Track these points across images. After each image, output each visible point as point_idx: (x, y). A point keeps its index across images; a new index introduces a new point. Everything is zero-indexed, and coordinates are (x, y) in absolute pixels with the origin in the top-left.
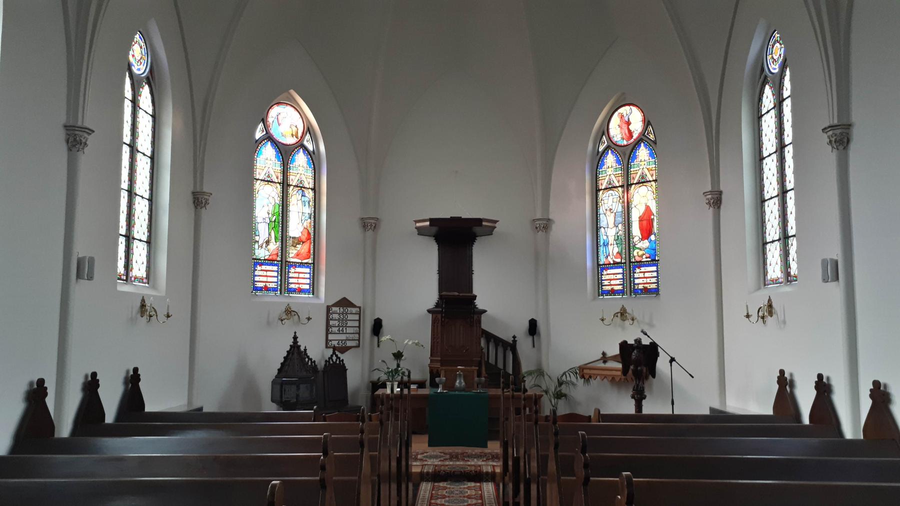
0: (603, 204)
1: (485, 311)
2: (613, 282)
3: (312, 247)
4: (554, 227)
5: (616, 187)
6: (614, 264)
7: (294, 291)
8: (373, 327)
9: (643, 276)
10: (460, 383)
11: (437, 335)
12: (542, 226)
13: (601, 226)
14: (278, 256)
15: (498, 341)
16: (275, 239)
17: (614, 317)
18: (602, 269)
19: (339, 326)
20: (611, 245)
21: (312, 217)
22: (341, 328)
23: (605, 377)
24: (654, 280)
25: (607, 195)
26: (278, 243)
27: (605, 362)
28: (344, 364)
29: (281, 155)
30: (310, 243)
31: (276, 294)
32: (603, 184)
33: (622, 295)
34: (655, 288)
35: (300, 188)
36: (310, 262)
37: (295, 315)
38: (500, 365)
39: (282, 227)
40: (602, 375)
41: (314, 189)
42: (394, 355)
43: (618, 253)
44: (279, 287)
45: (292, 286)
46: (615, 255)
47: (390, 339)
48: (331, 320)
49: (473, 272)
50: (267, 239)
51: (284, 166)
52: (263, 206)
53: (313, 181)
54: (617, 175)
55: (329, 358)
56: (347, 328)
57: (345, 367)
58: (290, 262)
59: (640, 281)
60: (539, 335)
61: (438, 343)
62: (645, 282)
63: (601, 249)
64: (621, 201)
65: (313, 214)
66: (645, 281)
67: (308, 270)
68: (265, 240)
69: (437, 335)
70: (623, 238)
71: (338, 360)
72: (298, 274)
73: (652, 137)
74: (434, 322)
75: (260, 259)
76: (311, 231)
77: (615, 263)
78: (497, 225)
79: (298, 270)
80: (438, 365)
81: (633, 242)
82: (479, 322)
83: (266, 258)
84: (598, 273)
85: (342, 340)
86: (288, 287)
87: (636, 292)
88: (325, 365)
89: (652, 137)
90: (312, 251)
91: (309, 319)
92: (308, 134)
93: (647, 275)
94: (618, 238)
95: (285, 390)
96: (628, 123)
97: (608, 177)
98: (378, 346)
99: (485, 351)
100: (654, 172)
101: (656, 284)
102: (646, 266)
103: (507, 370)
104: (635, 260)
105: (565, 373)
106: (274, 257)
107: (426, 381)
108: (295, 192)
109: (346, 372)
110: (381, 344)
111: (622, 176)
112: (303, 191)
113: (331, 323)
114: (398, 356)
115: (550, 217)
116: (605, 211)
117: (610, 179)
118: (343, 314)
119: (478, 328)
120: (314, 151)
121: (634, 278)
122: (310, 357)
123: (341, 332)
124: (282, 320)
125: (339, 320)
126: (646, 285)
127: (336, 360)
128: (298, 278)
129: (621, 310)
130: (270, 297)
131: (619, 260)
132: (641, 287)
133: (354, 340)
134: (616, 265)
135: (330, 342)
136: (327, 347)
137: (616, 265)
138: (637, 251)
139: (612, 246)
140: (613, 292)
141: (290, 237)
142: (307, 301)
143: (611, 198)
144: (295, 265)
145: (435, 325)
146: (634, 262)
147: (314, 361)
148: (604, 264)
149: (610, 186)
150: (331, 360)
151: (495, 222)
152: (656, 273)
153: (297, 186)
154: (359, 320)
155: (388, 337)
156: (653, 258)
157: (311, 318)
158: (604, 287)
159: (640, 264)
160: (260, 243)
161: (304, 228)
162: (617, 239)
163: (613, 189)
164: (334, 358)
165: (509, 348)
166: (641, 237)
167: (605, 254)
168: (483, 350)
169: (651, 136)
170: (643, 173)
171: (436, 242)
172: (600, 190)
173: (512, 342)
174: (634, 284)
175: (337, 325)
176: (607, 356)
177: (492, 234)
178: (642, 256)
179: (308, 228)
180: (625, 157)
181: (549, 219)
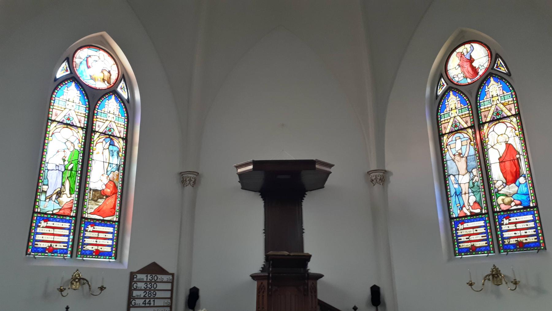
0: (449, 149)
1: (321, 276)
2: (472, 238)
3: (118, 202)
4: (391, 178)
5: (465, 129)
6: (471, 216)
7: (91, 253)
8: (188, 298)
12: (379, 178)
13: (450, 173)
14: (71, 211)
16: (70, 190)
17: (485, 280)
18: (456, 224)
19: (145, 297)
20: (465, 194)
21: (121, 168)
24: (531, 232)
25: (454, 139)
26: (73, 196)
29: (88, 98)
30: (116, 198)
31: (64, 256)
32: (447, 128)
35: (107, 136)
36: (115, 220)
37: (84, 284)
39: (81, 177)
41: (125, 139)
43: (475, 202)
45: (89, 248)
46: (471, 204)
48: (135, 289)
49: (304, 231)
50: (59, 189)
51: (89, 110)
52: (58, 152)
53: (125, 130)
54: (464, 116)
58: (87, 219)
59: (512, 234)
60: (384, 305)
62: (519, 235)
63: (453, 200)
64: (472, 143)
65: (122, 166)
66: (518, 233)
67: (111, 229)
68: (55, 192)
69: (263, 308)
70: (480, 184)
72: (97, 233)
73: (503, 70)
75: (46, 214)
77: (473, 214)
78: (332, 170)
79: (98, 228)
81: (495, 188)
82: (314, 290)
83: (55, 212)
84: (452, 228)
86: (82, 248)
87: (507, 248)
89: (503, 70)
90: (117, 208)
91: (102, 288)
92: (123, 82)
93: (519, 226)
96: (471, 60)
97: (452, 119)
100: (512, 106)
101: (536, 237)
104: (500, 209)
106: (67, 212)
108: (101, 140)
111: (470, 116)
112: (111, 139)
113: (135, 293)
115: (386, 169)
116: (453, 157)
117: (455, 122)
120: (128, 100)
121: (502, 231)
123: (147, 305)
124: (61, 291)
125: (145, 290)
126: (519, 239)
128: (97, 238)
129: (493, 271)
130: (56, 261)
131: (478, 211)
132: (513, 241)
134: (474, 217)
137: (474, 217)
139: (467, 195)
140: (474, 250)
141: (90, 189)
142: (109, 267)
143: (459, 142)
144: (94, 223)
145: (261, 293)
146: (499, 212)
148: (458, 217)
149: (456, 129)
151: (331, 166)
152: (533, 223)
153: (104, 134)
154: (172, 290)
156: (526, 204)
157: (105, 288)
158: (461, 245)
159: (508, 213)
161: (110, 180)
162: (472, 186)
163: (461, 131)
166: (505, 181)
167: (458, 205)
169: (502, 68)
170: (497, 109)
172: (443, 135)
174: (503, 239)
175: (142, 296)
177: (324, 187)
179: (115, 181)
180: (471, 96)
181: (386, 171)
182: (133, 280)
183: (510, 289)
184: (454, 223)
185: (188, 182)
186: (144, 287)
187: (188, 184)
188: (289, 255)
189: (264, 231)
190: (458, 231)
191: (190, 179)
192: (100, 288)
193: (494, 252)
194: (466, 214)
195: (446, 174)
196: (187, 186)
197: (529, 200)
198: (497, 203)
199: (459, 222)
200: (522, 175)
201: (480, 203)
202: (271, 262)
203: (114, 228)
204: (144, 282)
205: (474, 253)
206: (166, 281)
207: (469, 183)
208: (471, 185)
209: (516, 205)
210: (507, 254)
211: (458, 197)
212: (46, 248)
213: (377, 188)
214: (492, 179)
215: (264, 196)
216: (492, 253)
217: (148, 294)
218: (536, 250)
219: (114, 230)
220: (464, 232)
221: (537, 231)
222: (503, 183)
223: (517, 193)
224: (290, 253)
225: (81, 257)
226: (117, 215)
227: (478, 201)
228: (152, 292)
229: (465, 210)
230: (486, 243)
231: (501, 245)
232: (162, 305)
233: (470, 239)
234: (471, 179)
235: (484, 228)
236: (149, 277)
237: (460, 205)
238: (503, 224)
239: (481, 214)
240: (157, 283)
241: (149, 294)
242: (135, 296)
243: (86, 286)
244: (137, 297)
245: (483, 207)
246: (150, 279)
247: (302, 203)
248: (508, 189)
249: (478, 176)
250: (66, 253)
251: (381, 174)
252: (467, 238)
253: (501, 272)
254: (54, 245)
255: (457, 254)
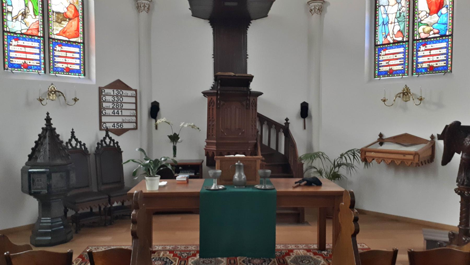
1: (261, 94)
2: (391, 63)
3: (81, 25)
6: (393, 43)
7: (62, 70)
8: (150, 110)
9: (429, 54)
10: (240, 176)
11: (213, 118)
12: (317, 8)
15: (271, 123)
16: (34, 12)
17: (396, 97)
18: (380, 51)
20: (392, 23)
22: (116, 111)
23: (383, 159)
26: (37, 17)
27: (381, 144)
28: (119, 146)
30: (78, 22)
33: (402, 76)
34: (443, 66)
36: (80, 41)
37: (60, 95)
38: (273, 146)
40: (379, 158)
42: (170, 137)
43: (399, 31)
44: (43, 66)
45: (60, 65)
46: (395, 33)
47: (166, 122)
48: (104, 102)
49: (248, 56)
50: (24, 10)
55: (102, 141)
56: (123, 111)
57: (120, 149)
58: (54, 39)
59: (425, 59)
60: (311, 117)
61: (213, 125)
62: (432, 60)
63: (380, 29)
66: (431, 58)
67: (77, 50)
69: (213, 118)
70: (406, 14)
71: (112, 142)
72: (65, 53)
74: (210, 104)
75: (15, 33)
76: (79, 8)
77: (395, 42)
79: (65, 48)
80: (214, 148)
81: (419, 18)
83: (23, 32)
84: (375, 54)
85: (118, 123)
86: (53, 66)
88: (97, 148)
90: (81, 30)
91: (76, 100)
93: (433, 52)
94: (400, 16)
95: (33, 181)
98: (156, 128)
99: (260, 133)
102: (434, 43)
103: (279, 151)
105: (342, 155)
106: (35, 32)
107: (203, 161)
109: (121, 155)
110: (159, 127)
113: (105, 105)
114: (174, 138)
118: (117, 96)
119: (254, 111)
122: (79, 140)
123: (116, 114)
124: (41, 100)
125: (113, 102)
126: (431, 64)
127: (110, 142)
128: (66, 57)
129: (404, 90)
130: (32, 76)
131: (400, 39)
132: (425, 65)
133: (131, 122)
135: (104, 125)
136: (101, 129)
138: (422, 27)
140: (391, 73)
141: (53, 12)
145: (211, 107)
146: (419, 40)
147: (84, 144)
148: (382, 45)
150: (103, 143)
154: (136, 103)
155: (163, 120)
156: (443, 33)
157: (78, 99)
159: (426, 41)
160: (14, 14)
161: (71, 4)
164: (108, 140)
165: (282, 130)
166: (428, 11)
167: (384, 33)
168: (258, 133)
171: (211, 25)
173: (284, 125)
175: (111, 107)
176: (384, 138)
177: (268, 16)
178: (428, 32)
179: (75, 4)
182: (102, 93)
183: (416, 105)
184: (378, 49)
185: (143, 8)
186: (112, 100)
187: (143, 10)
188: (234, 76)
189: (213, 56)
190: (380, 57)
191: (144, 4)
192: (74, 99)
193: (408, 75)
194: (389, 41)
195: (377, 4)
196: (142, 12)
197: (446, 28)
198: (418, 32)
199: (382, 48)
200: (445, 5)
201: (403, 32)
202: (219, 81)
203: (80, 48)
204: (111, 95)
205: (391, 75)
206: (130, 95)
207: (396, 13)
208: (398, 15)
209: (434, 34)
210: (418, 77)
211: (384, 26)
212: (21, 64)
213: (315, 17)
214: (417, 9)
215: (213, 23)
216: (406, 76)
217: (115, 105)
218: (443, 72)
219: (80, 50)
220: (386, 58)
221: (447, 57)
222: (427, 13)
223: (437, 23)
224: (235, 74)
225: (53, 73)
226: (81, 37)
227: (402, 30)
228: (119, 104)
229: (389, 38)
230: (402, 67)
231: (414, 69)
232: (129, 115)
233: (390, 64)
234: (398, 10)
235: (403, 54)
236: (116, 92)
237: (385, 34)
238: (419, 51)
239: (403, 42)
240: (123, 97)
241: (117, 105)
242: (105, 107)
243: (62, 97)
244: (106, 108)
245: (405, 36)
246: (116, 94)
247: (247, 31)
248: (430, 18)
249: (405, 7)
250: (40, 69)
251: (320, 4)
252: (386, 63)
253: (410, 91)
254: (27, 62)
255: (377, 77)
